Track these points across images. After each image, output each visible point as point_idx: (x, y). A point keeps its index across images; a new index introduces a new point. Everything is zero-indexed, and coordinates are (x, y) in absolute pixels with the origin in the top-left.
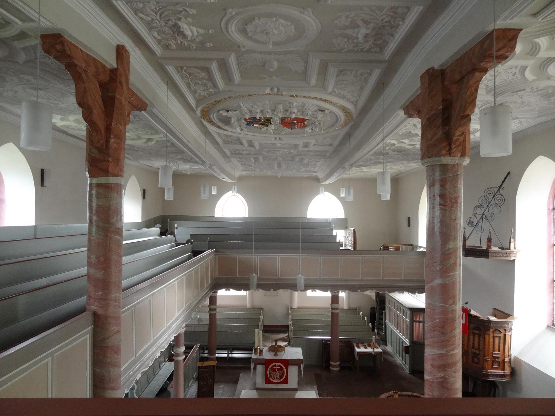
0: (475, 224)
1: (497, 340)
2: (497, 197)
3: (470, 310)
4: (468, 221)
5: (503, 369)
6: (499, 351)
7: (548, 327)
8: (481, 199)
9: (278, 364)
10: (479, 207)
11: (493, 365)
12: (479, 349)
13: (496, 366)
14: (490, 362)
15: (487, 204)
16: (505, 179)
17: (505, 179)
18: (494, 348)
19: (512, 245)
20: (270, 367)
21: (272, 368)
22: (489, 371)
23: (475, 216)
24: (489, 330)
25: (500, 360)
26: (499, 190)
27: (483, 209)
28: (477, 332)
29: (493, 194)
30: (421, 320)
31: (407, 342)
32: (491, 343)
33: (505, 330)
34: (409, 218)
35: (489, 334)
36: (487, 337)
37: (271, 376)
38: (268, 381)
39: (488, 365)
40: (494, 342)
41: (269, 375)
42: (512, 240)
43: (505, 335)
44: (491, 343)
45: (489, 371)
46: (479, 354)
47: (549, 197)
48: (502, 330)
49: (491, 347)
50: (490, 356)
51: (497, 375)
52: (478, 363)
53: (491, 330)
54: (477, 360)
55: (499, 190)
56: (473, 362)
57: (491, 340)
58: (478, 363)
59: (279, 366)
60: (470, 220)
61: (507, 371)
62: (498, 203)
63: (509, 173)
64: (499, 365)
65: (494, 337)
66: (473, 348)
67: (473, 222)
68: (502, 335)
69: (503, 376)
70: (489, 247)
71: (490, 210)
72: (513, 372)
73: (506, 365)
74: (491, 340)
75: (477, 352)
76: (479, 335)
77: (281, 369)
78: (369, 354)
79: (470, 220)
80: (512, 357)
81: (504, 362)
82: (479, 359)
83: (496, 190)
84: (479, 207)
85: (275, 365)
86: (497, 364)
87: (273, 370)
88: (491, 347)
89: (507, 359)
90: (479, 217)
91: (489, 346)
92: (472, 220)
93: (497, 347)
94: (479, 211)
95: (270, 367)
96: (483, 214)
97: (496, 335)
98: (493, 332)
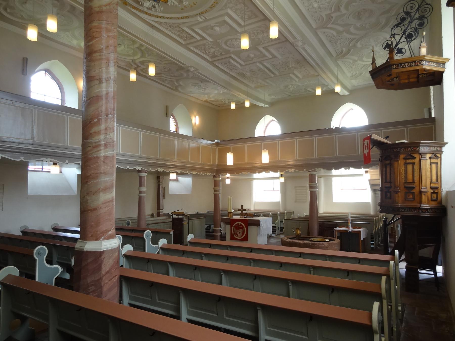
1: (410, 167)
4: (385, 45)
8: (399, 17)
9: (240, 223)
10: (397, 25)
12: (391, 182)
18: (406, 177)
20: (234, 225)
21: (235, 226)
23: (394, 37)
28: (388, 162)
36: (396, 164)
37: (235, 234)
38: (232, 238)
40: (406, 171)
41: (233, 233)
43: (420, 160)
48: (416, 155)
53: (402, 156)
58: (390, 198)
59: (241, 225)
65: (406, 164)
77: (242, 228)
80: (444, 193)
82: (390, 192)
84: (397, 25)
85: (238, 224)
86: (411, 196)
87: (236, 228)
92: (390, 43)
93: (410, 177)
95: (234, 225)
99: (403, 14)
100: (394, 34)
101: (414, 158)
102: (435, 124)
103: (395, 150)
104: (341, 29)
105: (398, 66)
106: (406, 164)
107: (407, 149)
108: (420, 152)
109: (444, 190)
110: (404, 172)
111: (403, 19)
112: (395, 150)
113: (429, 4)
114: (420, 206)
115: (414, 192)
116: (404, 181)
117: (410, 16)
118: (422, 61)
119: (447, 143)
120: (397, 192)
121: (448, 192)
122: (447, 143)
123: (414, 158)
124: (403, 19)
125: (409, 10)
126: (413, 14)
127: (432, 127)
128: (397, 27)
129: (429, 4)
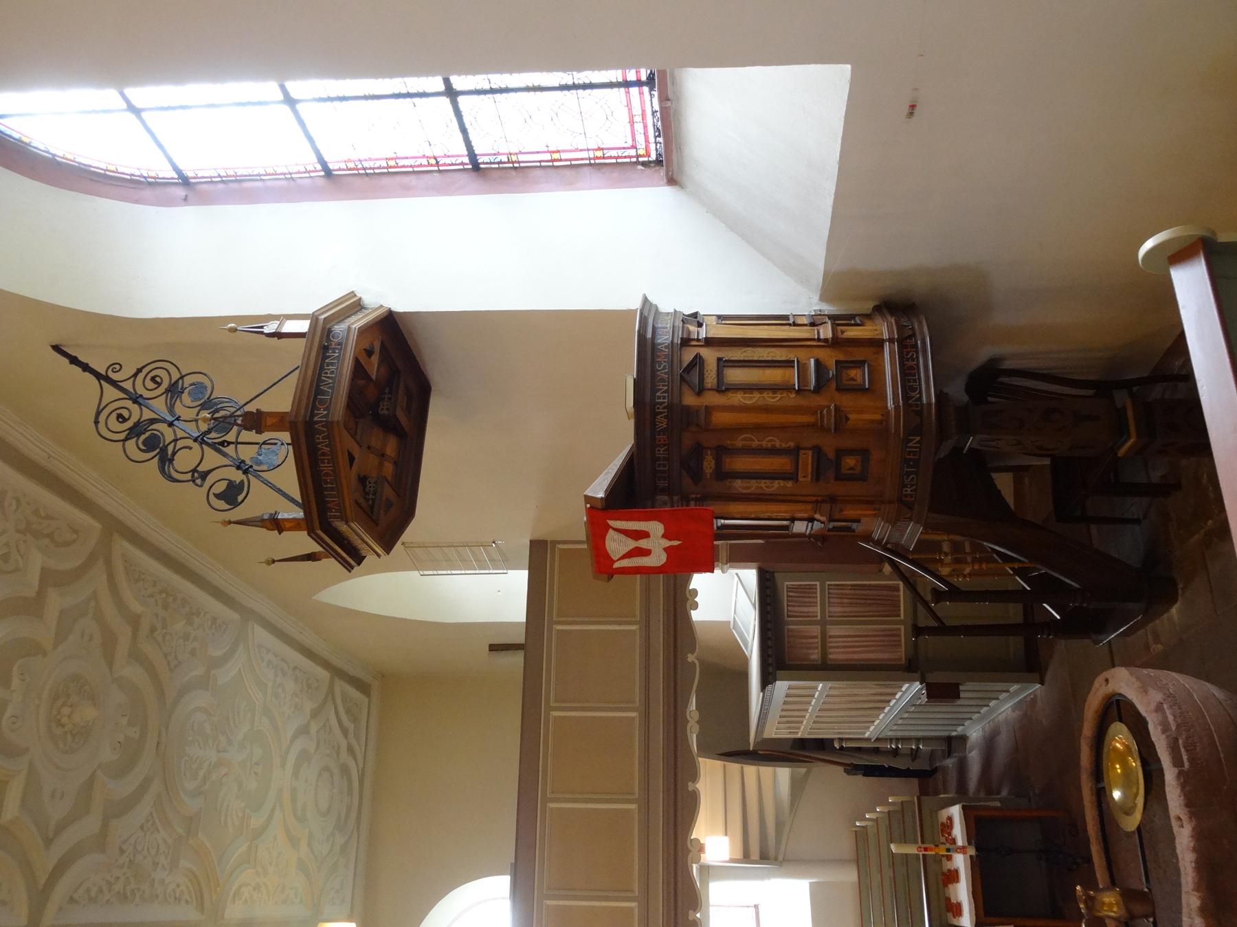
0: (238, 476)
1: (735, 375)
2: (140, 390)
3: (588, 499)
4: (222, 504)
5: (877, 344)
6: (788, 364)
7: (672, 181)
10: (166, 460)
11: (861, 390)
12: (794, 452)
13: (861, 376)
14: (847, 401)
15: (162, 427)
16: (74, 360)
17: (74, 360)
18: (774, 388)
19: (290, 327)
22: (890, 404)
23: (204, 476)
24: (687, 410)
25: (830, 358)
26: (114, 383)
27: (180, 444)
28: (709, 464)
29: (129, 404)
30: (816, 630)
31: (912, 690)
32: (754, 399)
33: (686, 342)
34: (494, 648)
35: (709, 410)
36: (721, 418)
39: (861, 413)
42: (271, 328)
43: (710, 342)
44: (754, 399)
45: (890, 404)
46: (817, 450)
47: (137, 202)
48: (688, 355)
49: (770, 399)
50: (819, 400)
51: (908, 372)
52: (864, 453)
53: (690, 400)
54: (850, 462)
55: (114, 383)
56: (862, 478)
57: (738, 398)
58: (864, 453)
60: (217, 496)
61: (882, 328)
62: (165, 385)
63: (57, 348)
64: (859, 364)
66: (793, 476)
67: (231, 484)
68: (710, 355)
69: (906, 344)
70: (280, 421)
71: (191, 414)
72: (896, 305)
73: (852, 333)
74: (738, 398)
75: (807, 458)
76: (722, 451)
78: (980, 869)
79: (217, 496)
80: (827, 309)
81: (835, 343)
82: (841, 453)
83: (111, 393)
84: (166, 460)
88: (770, 399)
89: (826, 332)
90: (212, 459)
91: (767, 409)
94: (185, 460)
96: (203, 442)
97: (711, 379)
98: (701, 391)
99: (131, 444)
100: (194, 471)
101: (698, 361)
102: (554, 543)
103: (662, 423)
104: (90, 825)
105: (322, 402)
106: (722, 388)
107: (662, 380)
108: (678, 341)
109: (817, 308)
110: (756, 395)
111: (152, 444)
112: (662, 423)
113: (139, 371)
114: (891, 340)
115: (837, 362)
116: (793, 395)
117: (153, 421)
118: (330, 331)
119: (646, 300)
120: (841, 416)
121: (824, 297)
122: (646, 300)
123: (698, 361)
124: (152, 444)
125: (129, 424)
126: (148, 415)
127: (561, 550)
128: (171, 460)
129: (139, 371)
